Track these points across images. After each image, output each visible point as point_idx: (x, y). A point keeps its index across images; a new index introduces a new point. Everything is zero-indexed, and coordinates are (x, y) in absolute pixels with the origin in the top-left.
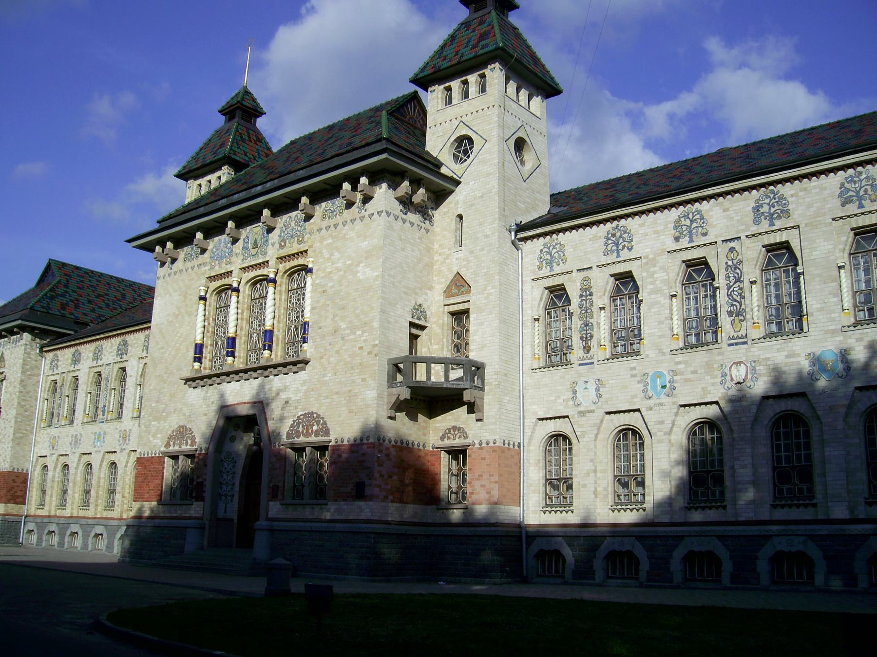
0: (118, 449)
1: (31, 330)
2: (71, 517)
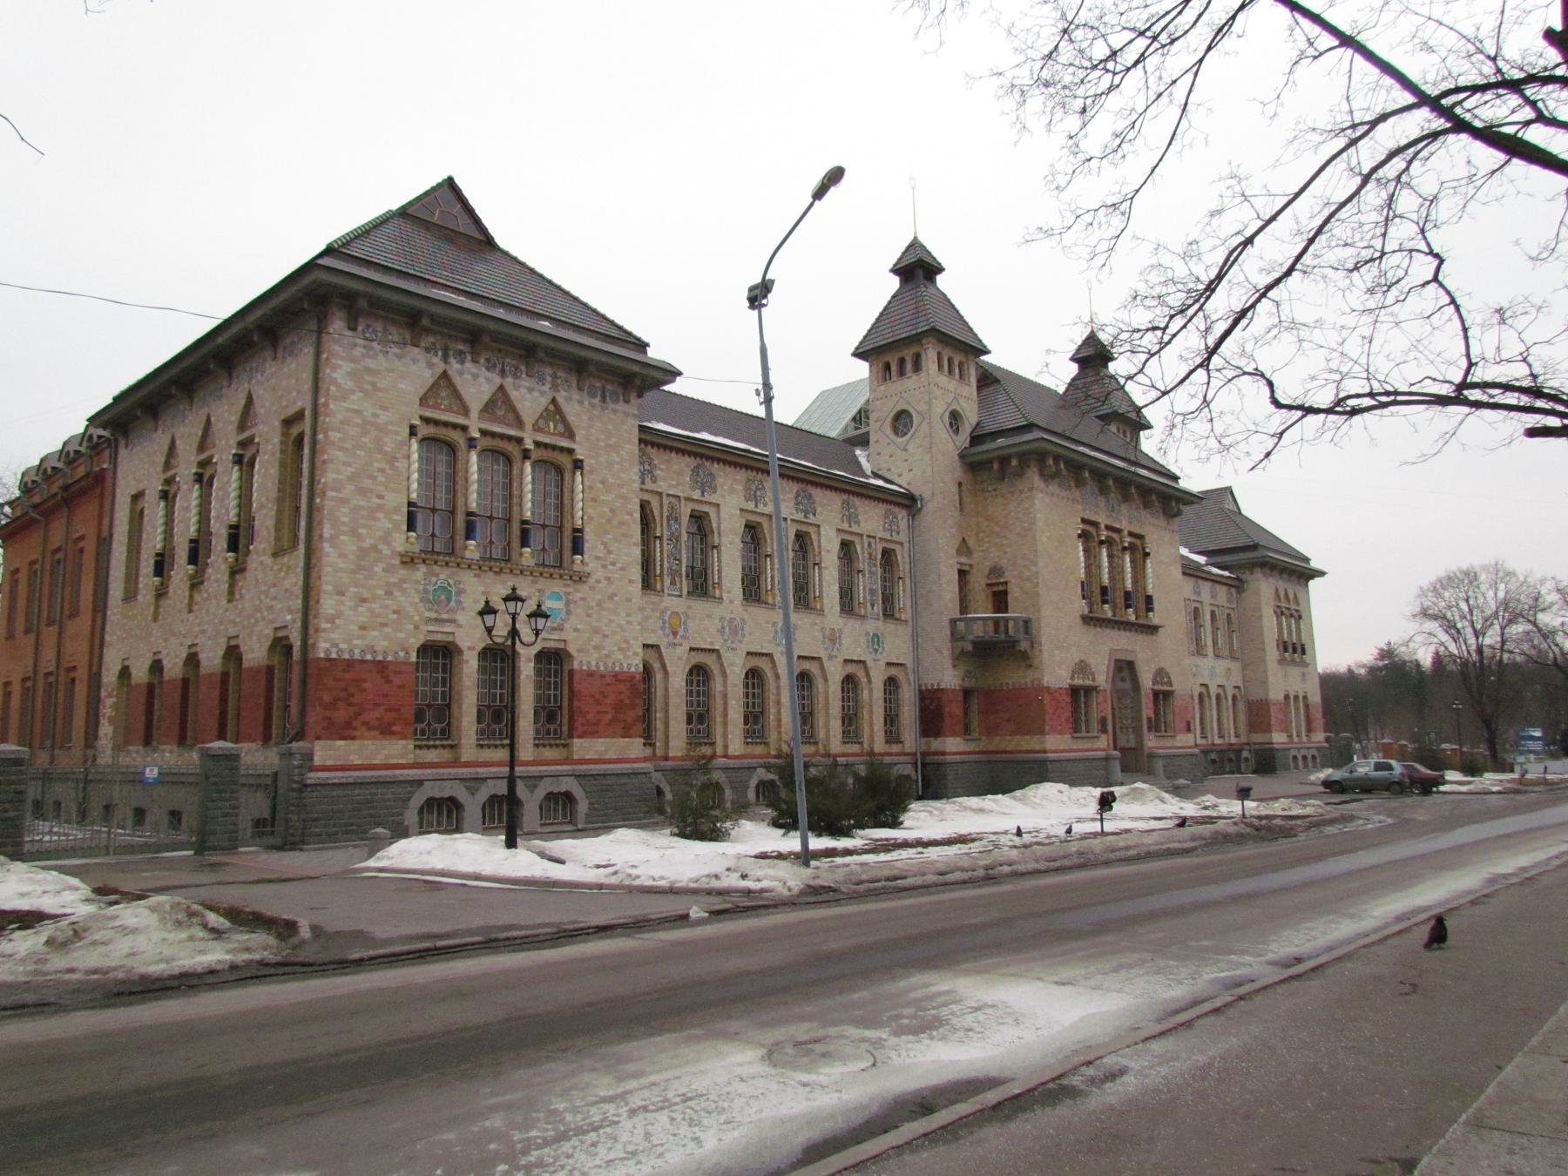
0: (823, 654)
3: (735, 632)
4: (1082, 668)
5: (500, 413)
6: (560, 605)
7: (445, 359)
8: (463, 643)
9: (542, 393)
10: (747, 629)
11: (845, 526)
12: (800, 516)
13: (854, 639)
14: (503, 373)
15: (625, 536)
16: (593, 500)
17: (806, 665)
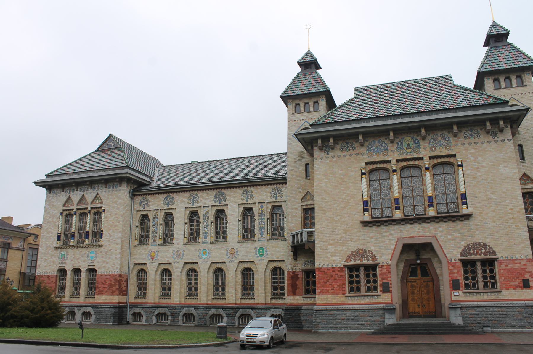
2: (180, 304)
4: (361, 253)
5: (84, 202)
6: (94, 255)
7: (70, 193)
8: (67, 269)
9: (94, 193)
10: (185, 254)
13: (247, 252)
15: (116, 230)
16: (107, 221)
17: (219, 266)
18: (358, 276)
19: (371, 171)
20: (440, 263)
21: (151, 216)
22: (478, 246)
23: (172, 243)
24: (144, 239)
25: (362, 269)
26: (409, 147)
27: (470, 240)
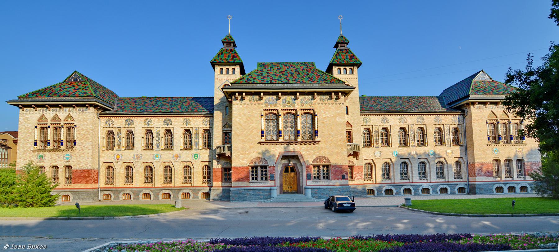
1: (95, 106)
3: (138, 158)
10: (143, 156)
11: (185, 126)
12: (166, 126)
14: (56, 111)
18: (256, 171)
19: (267, 114)
20: (301, 165)
21: (115, 132)
22: (321, 158)
23: (133, 149)
24: (111, 147)
25: (259, 168)
26: (289, 102)
27: (318, 155)
